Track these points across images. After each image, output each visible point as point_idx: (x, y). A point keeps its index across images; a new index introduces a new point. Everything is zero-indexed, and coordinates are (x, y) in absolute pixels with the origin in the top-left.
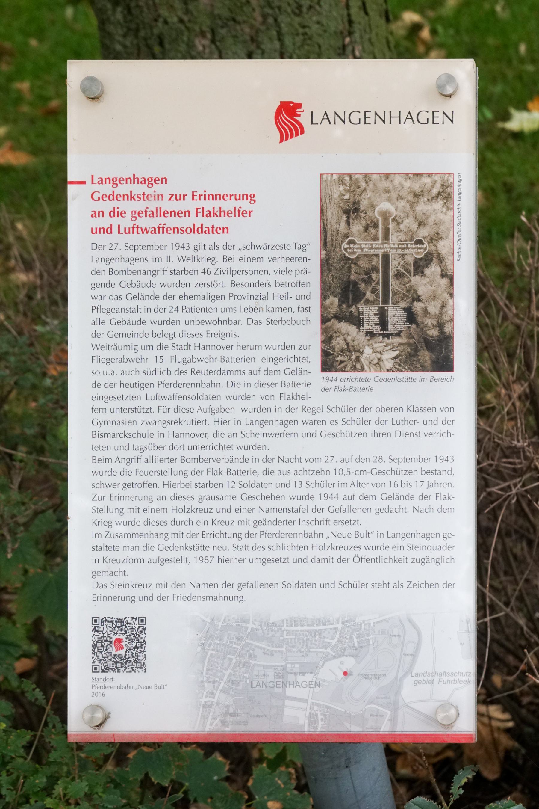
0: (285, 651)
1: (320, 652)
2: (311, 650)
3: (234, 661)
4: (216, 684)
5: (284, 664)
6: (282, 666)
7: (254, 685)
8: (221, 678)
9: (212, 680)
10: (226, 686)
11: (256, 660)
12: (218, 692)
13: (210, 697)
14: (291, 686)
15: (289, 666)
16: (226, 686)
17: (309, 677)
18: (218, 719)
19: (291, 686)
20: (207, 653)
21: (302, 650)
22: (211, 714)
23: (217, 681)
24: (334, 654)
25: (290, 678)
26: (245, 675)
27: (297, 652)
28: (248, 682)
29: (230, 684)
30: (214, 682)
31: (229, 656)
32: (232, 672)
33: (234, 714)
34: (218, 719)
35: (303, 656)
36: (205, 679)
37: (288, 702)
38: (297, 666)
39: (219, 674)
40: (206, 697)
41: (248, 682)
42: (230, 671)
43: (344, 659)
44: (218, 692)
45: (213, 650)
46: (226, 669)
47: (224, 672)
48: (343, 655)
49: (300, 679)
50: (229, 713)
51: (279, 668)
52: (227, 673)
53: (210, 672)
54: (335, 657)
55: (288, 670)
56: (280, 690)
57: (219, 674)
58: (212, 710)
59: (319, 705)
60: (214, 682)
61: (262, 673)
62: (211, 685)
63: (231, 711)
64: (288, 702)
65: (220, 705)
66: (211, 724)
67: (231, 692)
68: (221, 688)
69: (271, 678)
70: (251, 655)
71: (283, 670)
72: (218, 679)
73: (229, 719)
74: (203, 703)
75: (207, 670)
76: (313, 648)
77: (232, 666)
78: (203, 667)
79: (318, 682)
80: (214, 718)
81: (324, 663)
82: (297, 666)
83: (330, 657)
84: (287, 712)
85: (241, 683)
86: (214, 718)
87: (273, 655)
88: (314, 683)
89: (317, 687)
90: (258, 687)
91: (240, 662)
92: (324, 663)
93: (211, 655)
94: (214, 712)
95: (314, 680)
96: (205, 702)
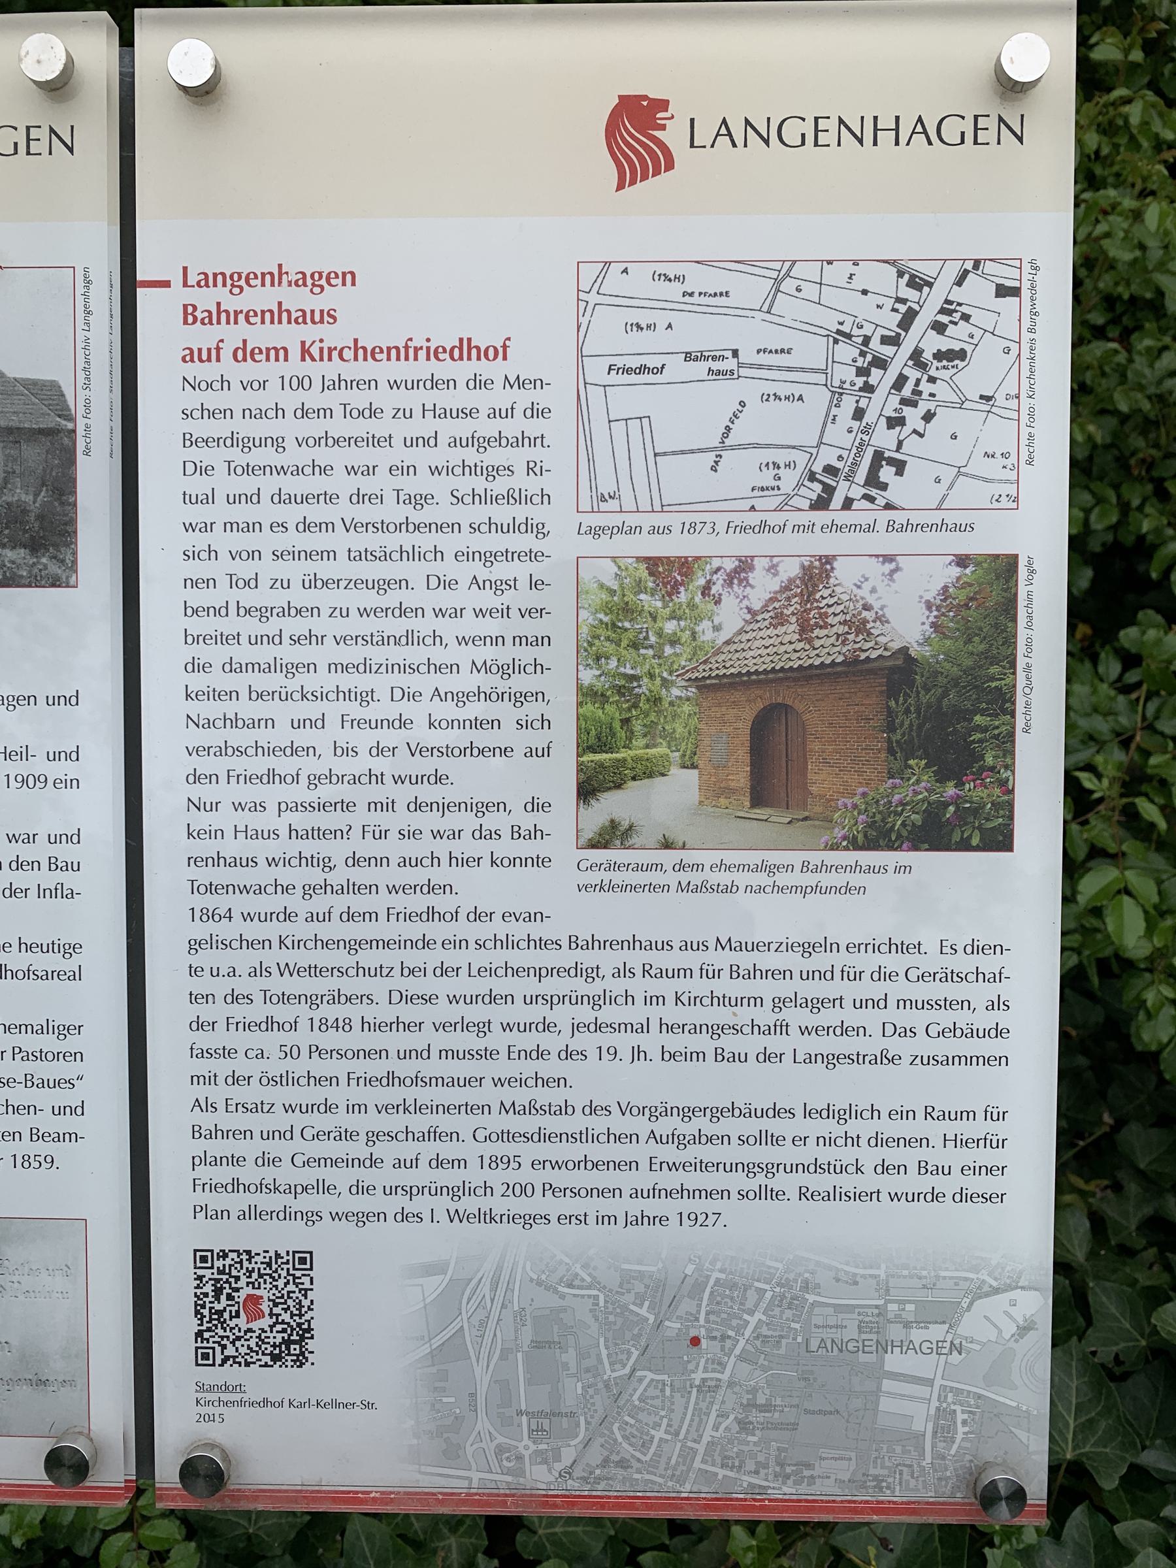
0: (883, 1276)
1: (966, 1279)
2: (943, 1274)
3: (769, 1295)
4: (728, 1343)
5: (882, 1302)
6: (877, 1307)
7: (814, 1344)
8: (739, 1330)
9: (718, 1334)
10: (749, 1347)
11: (819, 1294)
12: (733, 1359)
13: (714, 1371)
14: (897, 1350)
15: (892, 1307)
16: (749, 1347)
17: (937, 1332)
18: (732, 1417)
19: (897, 1350)
20: (708, 1277)
21: (924, 1273)
22: (715, 1407)
23: (729, 1337)
24: (995, 1284)
25: (895, 1332)
26: (793, 1325)
27: (911, 1277)
28: (799, 1339)
29: (758, 1343)
30: (724, 1337)
31: (757, 1284)
32: (764, 1318)
33: (767, 1408)
34: (732, 1417)
35: (924, 1287)
36: (703, 1332)
37: (887, 1385)
38: (910, 1307)
39: (734, 1322)
40: (706, 1370)
41: (799, 1339)
42: (759, 1316)
43: (1016, 1294)
44: (733, 1359)
45: (721, 1271)
46: (751, 1313)
47: (746, 1317)
48: (1017, 1288)
49: (917, 1335)
50: (755, 1406)
51: (869, 1311)
52: (753, 1321)
53: (712, 1317)
54: (996, 1291)
55: (890, 1316)
56: (872, 1358)
57: (734, 1322)
58: (719, 1398)
59: (957, 1392)
60: (724, 1337)
61: (832, 1321)
62: (715, 1343)
63: (761, 1400)
64: (887, 1385)
65: (737, 1389)
66: (716, 1428)
67: (761, 1361)
68: (737, 1351)
69: (851, 1332)
70: (806, 1282)
71: (879, 1315)
72: (731, 1333)
73: (756, 1417)
74: (697, 1383)
75: (708, 1313)
76: (947, 1269)
77: (763, 1305)
78: (699, 1306)
79: (956, 1342)
80: (723, 1415)
81: (971, 1304)
82: (910, 1307)
83: (986, 1289)
84: (885, 1404)
85: (784, 1341)
86: (723, 1415)
87: (856, 1283)
88: (947, 1345)
89: (955, 1353)
90: (822, 1352)
91: (783, 1297)
92: (971, 1304)
93: (718, 1280)
94: (723, 1402)
95: (949, 1338)
96: (704, 1380)
